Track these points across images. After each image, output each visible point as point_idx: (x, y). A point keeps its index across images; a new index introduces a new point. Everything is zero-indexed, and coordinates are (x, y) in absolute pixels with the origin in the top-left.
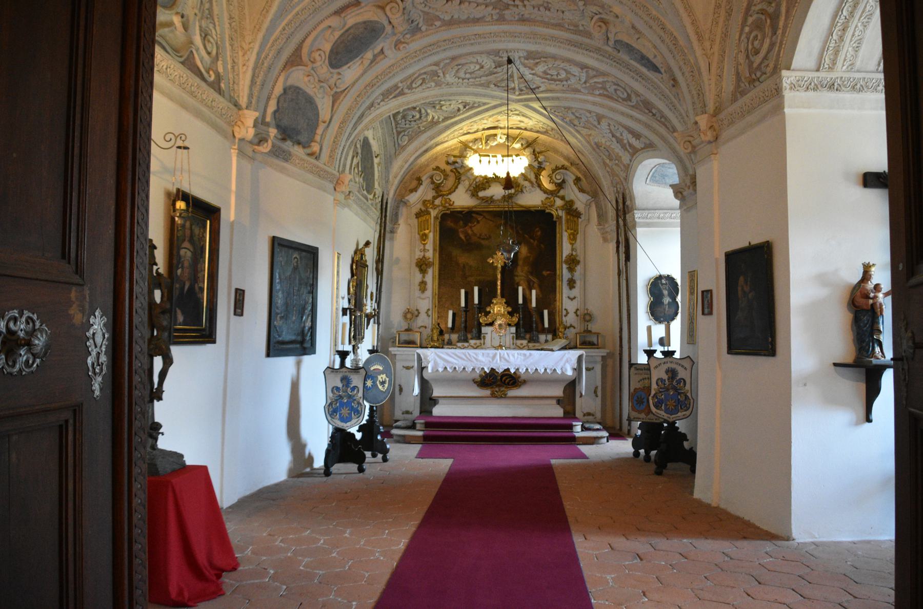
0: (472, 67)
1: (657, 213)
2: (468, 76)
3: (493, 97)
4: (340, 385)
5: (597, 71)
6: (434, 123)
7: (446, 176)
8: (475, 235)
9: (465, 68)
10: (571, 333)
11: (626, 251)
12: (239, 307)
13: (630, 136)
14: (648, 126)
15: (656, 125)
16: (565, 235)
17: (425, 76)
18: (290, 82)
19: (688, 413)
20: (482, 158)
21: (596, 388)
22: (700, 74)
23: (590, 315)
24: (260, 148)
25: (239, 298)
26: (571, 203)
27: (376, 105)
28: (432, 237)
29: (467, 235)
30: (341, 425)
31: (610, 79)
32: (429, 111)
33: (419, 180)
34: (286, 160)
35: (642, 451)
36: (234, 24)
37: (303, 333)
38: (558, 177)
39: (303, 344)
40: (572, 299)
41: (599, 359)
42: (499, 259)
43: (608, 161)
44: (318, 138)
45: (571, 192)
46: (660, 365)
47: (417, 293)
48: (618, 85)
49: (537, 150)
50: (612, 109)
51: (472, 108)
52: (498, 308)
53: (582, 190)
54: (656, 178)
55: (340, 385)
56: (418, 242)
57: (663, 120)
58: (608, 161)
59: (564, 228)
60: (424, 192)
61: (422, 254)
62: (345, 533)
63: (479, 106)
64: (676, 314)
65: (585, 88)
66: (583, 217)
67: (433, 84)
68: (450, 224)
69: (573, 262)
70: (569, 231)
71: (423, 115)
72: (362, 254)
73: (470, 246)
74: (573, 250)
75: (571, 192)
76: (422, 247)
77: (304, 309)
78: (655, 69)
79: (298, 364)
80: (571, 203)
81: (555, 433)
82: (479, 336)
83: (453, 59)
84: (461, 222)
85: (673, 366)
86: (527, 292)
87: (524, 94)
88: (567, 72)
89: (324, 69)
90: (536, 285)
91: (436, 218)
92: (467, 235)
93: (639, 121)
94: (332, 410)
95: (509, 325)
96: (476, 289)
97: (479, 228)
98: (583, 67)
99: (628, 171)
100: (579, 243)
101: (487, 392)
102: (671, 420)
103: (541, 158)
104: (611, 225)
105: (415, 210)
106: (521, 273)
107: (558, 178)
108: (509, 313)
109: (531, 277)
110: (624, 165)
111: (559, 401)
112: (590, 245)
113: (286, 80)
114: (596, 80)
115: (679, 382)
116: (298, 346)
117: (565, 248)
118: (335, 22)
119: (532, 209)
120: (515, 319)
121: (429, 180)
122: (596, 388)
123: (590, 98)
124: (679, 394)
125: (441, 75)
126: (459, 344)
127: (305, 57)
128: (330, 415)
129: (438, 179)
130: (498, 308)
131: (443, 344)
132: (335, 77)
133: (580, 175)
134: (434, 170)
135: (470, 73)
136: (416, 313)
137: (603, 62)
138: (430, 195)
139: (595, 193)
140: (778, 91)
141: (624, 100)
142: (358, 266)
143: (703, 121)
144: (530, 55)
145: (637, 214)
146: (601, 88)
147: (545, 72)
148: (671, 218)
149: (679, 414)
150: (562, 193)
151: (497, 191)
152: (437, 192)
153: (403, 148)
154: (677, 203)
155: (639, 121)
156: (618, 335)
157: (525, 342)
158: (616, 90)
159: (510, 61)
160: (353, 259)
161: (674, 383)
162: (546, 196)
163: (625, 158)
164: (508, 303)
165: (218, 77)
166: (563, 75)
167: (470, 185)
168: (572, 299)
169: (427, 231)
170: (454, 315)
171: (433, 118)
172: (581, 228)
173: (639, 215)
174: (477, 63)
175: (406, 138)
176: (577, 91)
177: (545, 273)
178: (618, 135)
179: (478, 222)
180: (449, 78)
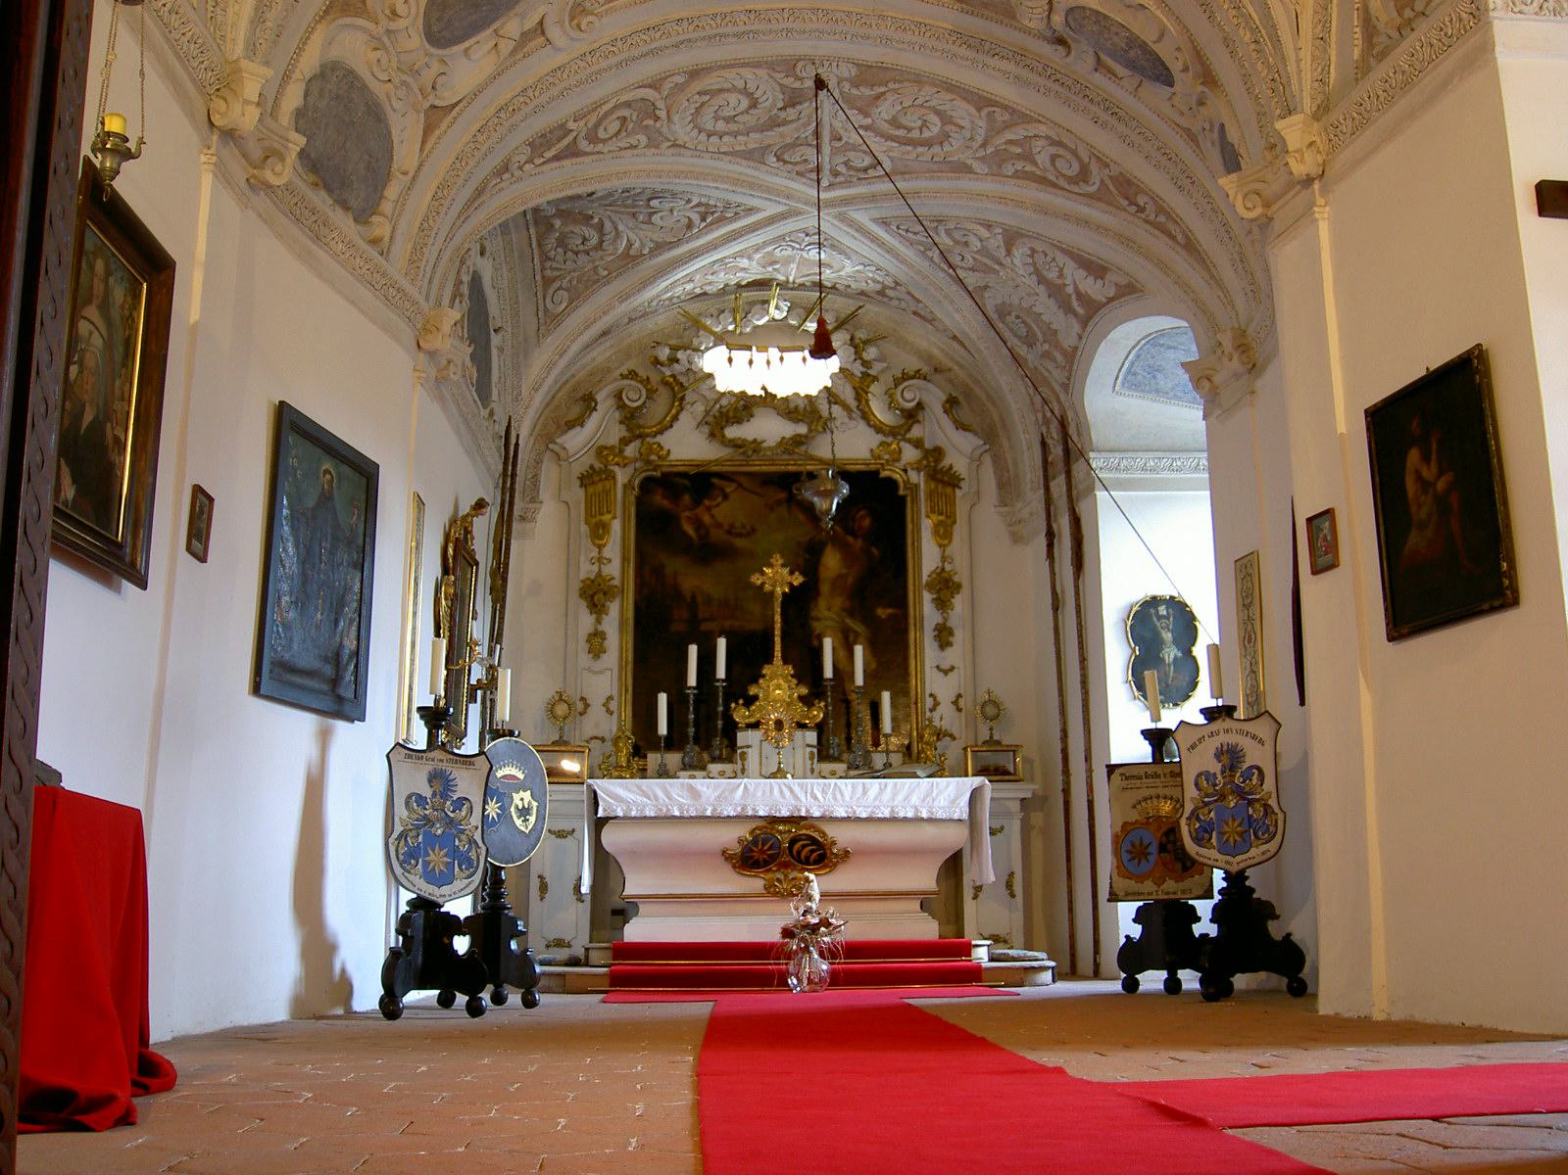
0: (733, 98)
1: (1141, 459)
2: (721, 126)
3: (769, 190)
4: (427, 792)
5: (1013, 111)
6: (630, 259)
7: (651, 393)
8: (720, 525)
9: (719, 100)
11: (1073, 549)
13: (1082, 273)
15: (1143, 235)
16: (927, 525)
17: (625, 113)
18: (334, 54)
19: (1272, 846)
20: (735, 354)
21: (1012, 874)
22: (1276, 41)
25: (201, 506)
27: (514, 167)
28: (619, 531)
29: (698, 524)
30: (430, 891)
31: (1043, 130)
32: (621, 227)
33: (589, 403)
34: (317, 238)
37: (336, 659)
38: (908, 395)
40: (946, 672)
41: (1015, 806)
42: (777, 577)
44: (387, 207)
45: (937, 429)
46: (1201, 740)
47: (585, 659)
48: (1060, 144)
49: (861, 335)
50: (1043, 210)
51: (722, 220)
52: (778, 687)
53: (961, 426)
54: (1139, 378)
55: (427, 792)
56: (587, 542)
57: (1164, 222)
59: (923, 508)
60: (602, 426)
61: (595, 568)
64: (1194, 685)
65: (982, 159)
67: (643, 139)
68: (659, 499)
69: (945, 587)
70: (935, 518)
72: (467, 532)
73: (708, 551)
74: (944, 559)
75: (937, 429)
76: (595, 553)
77: (341, 603)
79: (324, 738)
80: (938, 453)
83: (694, 74)
84: (687, 498)
88: (946, 119)
92: (698, 524)
93: (1101, 229)
95: (801, 726)
96: (722, 644)
97: (727, 510)
98: (982, 102)
99: (1074, 362)
100: (957, 547)
101: (755, 884)
105: (579, 467)
106: (827, 610)
107: (908, 397)
108: (801, 698)
109: (848, 621)
113: (329, 43)
114: (1009, 136)
115: (1247, 776)
117: (927, 555)
121: (611, 401)
123: (989, 186)
124: (1251, 803)
125: (663, 114)
129: (634, 397)
130: (778, 687)
132: (436, 67)
135: (728, 120)
136: (580, 706)
137: (1027, 83)
138: (615, 434)
139: (991, 435)
141: (1072, 180)
142: (457, 558)
144: (869, 74)
145: (1097, 461)
146: (1020, 157)
147: (894, 122)
148: (1170, 469)
149: (1253, 852)
150: (916, 432)
151: (769, 429)
152: (629, 430)
155: (1101, 229)
156: (1059, 746)
157: (841, 767)
158: (1053, 158)
159: (820, 84)
160: (447, 537)
161: (1238, 780)
162: (880, 438)
163: (1067, 328)
164: (799, 678)
166: (935, 127)
167: (707, 413)
168: (946, 672)
169: (607, 517)
171: (630, 245)
172: (961, 509)
173: (1100, 464)
174: (745, 92)
176: (963, 169)
177: (882, 612)
178: (1052, 275)
179: (726, 497)
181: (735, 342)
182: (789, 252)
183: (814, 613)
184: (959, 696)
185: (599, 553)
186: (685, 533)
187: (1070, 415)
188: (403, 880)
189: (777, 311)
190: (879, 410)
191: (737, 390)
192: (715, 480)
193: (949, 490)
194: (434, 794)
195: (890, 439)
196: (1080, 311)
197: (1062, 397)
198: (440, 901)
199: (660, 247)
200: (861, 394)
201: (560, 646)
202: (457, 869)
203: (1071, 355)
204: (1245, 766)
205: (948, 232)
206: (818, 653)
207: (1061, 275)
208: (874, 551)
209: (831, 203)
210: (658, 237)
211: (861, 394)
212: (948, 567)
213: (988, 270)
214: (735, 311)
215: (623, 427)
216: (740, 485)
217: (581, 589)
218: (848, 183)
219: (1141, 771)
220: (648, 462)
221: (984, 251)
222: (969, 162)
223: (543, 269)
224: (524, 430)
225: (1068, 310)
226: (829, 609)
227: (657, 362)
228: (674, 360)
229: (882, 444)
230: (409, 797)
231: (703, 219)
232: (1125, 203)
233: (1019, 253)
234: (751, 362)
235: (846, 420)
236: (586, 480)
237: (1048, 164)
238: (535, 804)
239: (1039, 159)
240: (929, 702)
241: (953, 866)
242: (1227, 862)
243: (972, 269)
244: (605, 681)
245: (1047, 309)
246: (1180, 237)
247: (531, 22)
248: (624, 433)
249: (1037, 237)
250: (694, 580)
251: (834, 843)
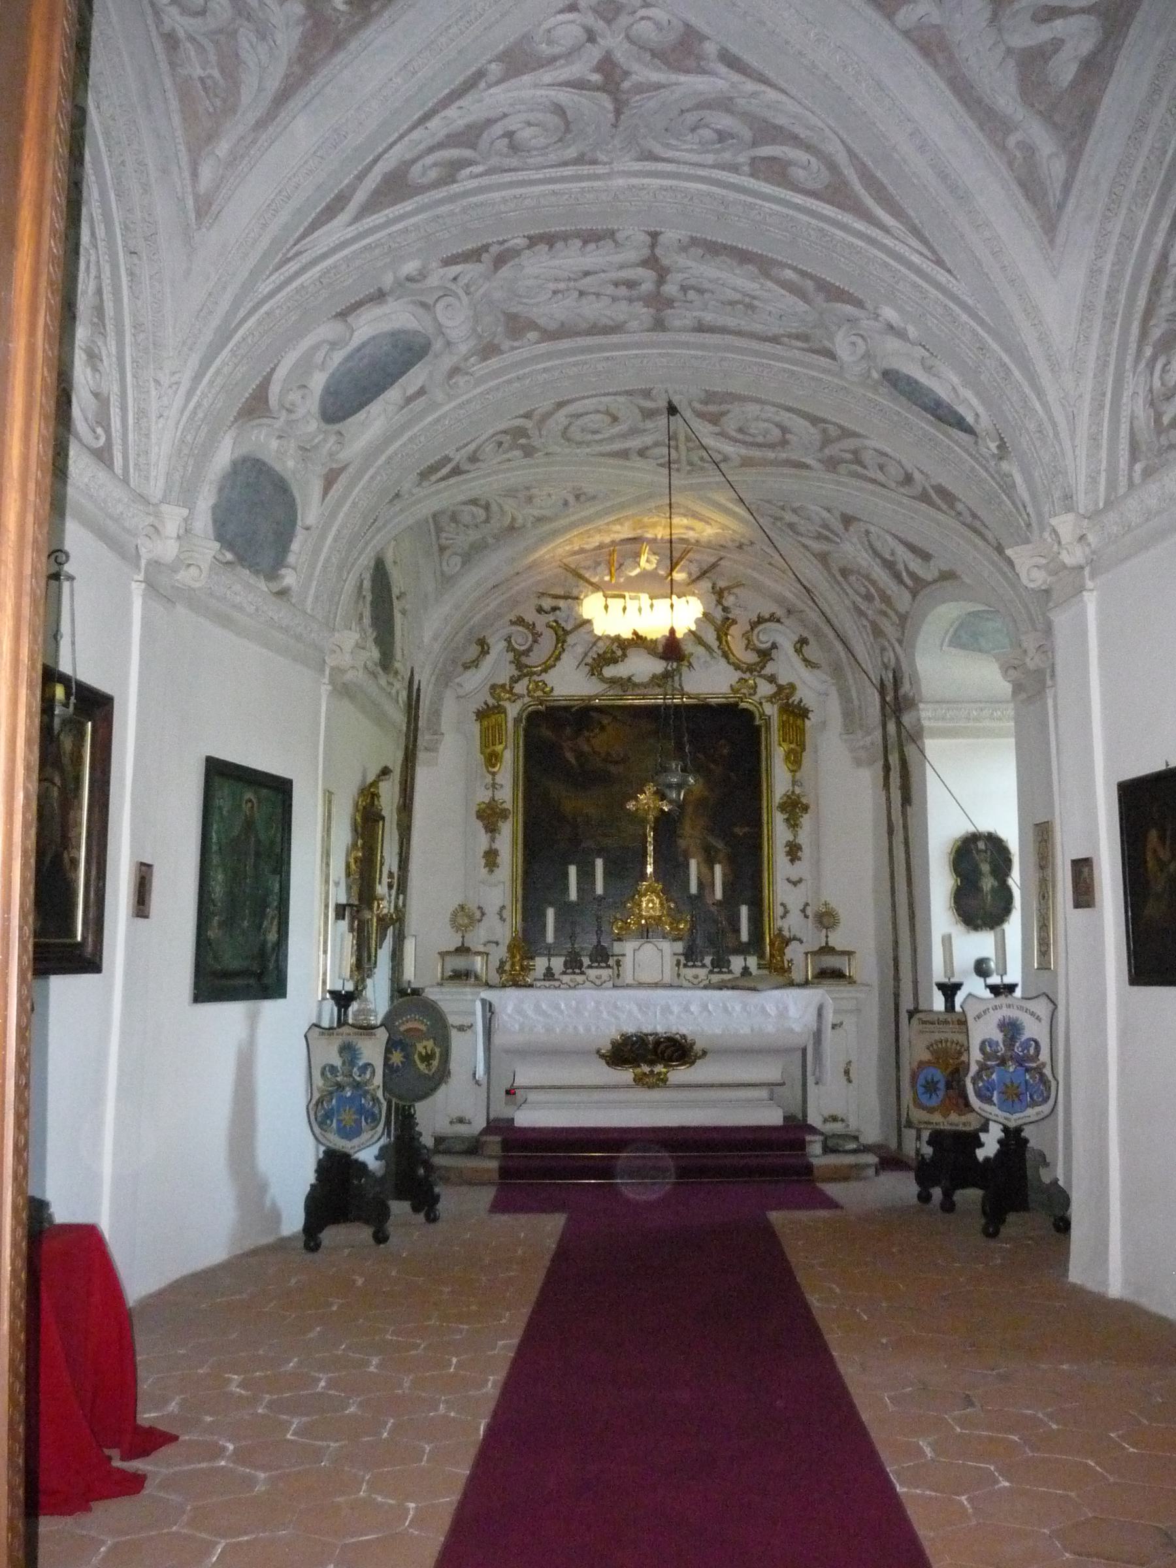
4: (337, 1062)
7: (536, 636)
16: (779, 753)
19: (1045, 1109)
29: (580, 755)
30: (340, 1144)
32: (506, 508)
33: (484, 647)
36: (142, 336)
40: (795, 884)
49: (722, 584)
55: (337, 1062)
58: (864, 606)
60: (496, 667)
61: (489, 793)
62: (367, 1363)
64: (1007, 910)
68: (546, 733)
69: (794, 807)
70: (786, 746)
72: (374, 796)
73: (588, 777)
74: (794, 783)
76: (489, 779)
79: (253, 1020)
85: (1014, 1013)
86: (705, 870)
91: (517, 721)
92: (580, 755)
94: (322, 1114)
101: (626, 1075)
102: (1012, 1124)
103: (729, 601)
105: (477, 704)
115: (1025, 1045)
116: (252, 981)
117: (779, 780)
121: (504, 644)
127: (273, 401)
133: (805, 635)
134: (512, 623)
136: (478, 914)
142: (367, 820)
145: (926, 714)
148: (992, 718)
150: (769, 669)
151: (642, 667)
154: (1005, 688)
159: (672, 410)
162: (738, 674)
168: (795, 884)
169: (499, 748)
171: (513, 519)
173: (929, 714)
177: (739, 831)
179: (603, 728)
181: (612, 591)
182: (655, 519)
184: (807, 904)
185: (493, 779)
189: (647, 562)
191: (612, 635)
192: (593, 714)
193: (799, 722)
194: (344, 1063)
195: (747, 676)
198: (352, 1152)
201: (458, 867)
202: (364, 1123)
203: (903, 618)
204: (1024, 1038)
207: (893, 554)
210: (536, 512)
212: (798, 790)
214: (612, 566)
215: (513, 666)
216: (615, 718)
217: (478, 811)
223: (438, 538)
224: (425, 678)
225: (901, 581)
229: (741, 679)
230: (324, 1068)
234: (624, 609)
235: (708, 659)
236: (481, 715)
240: (780, 911)
242: (1006, 1118)
244: (499, 892)
245: (881, 575)
250: (574, 803)
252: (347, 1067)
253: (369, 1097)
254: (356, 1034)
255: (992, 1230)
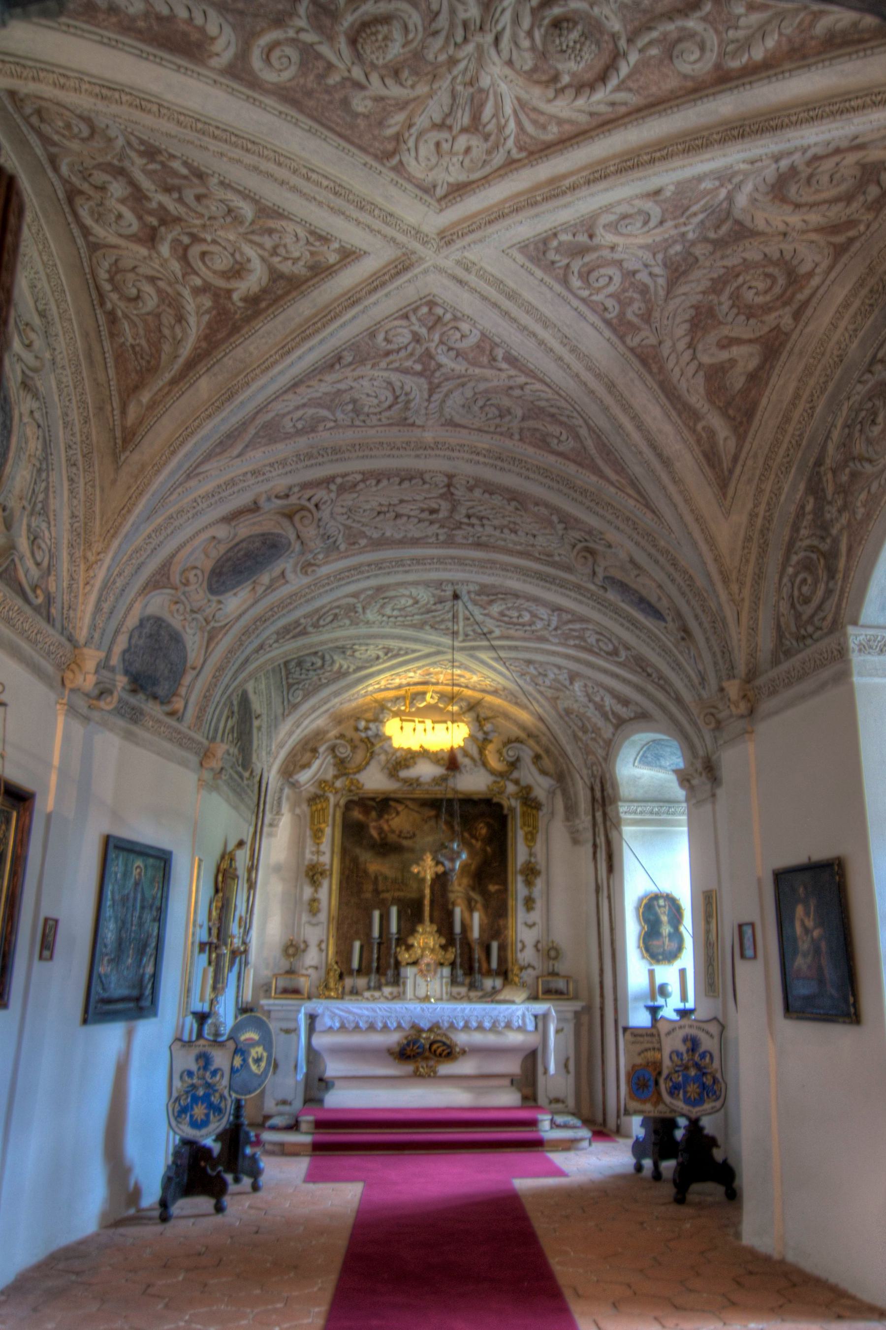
0: (403, 601)
2: (396, 613)
3: (426, 642)
4: (194, 1067)
6: (342, 674)
8: (393, 832)
10: (528, 975)
12: (47, 944)
14: (641, 690)
15: (650, 688)
16: (521, 834)
17: (337, 611)
20: (405, 724)
23: (557, 950)
24: (102, 704)
26: (529, 788)
27: (266, 647)
28: (331, 834)
31: (590, 626)
32: (335, 657)
35: (648, 1163)
39: (139, 1003)
41: (570, 1016)
43: (580, 734)
44: (183, 691)
45: (529, 774)
48: (601, 634)
49: (482, 715)
52: (426, 939)
53: (543, 772)
54: (649, 757)
55: (194, 1067)
58: (580, 734)
59: (519, 822)
63: (406, 654)
64: (680, 948)
65: (555, 636)
66: (545, 809)
68: (357, 814)
69: (531, 872)
70: (526, 829)
71: (328, 663)
73: (386, 848)
74: (531, 855)
75: (529, 774)
77: (145, 945)
78: (657, 614)
79: (130, 1035)
80: (529, 788)
81: (511, 1136)
82: (397, 980)
83: (379, 589)
84: (374, 814)
86: (466, 915)
87: (470, 640)
88: (534, 615)
89: (198, 594)
90: (479, 906)
91: (337, 805)
92: (381, 830)
93: (625, 681)
94: (181, 1110)
95: (442, 964)
96: (394, 910)
97: (399, 822)
99: (610, 749)
100: (539, 847)
101: (409, 1068)
103: (488, 727)
104: (584, 820)
110: (604, 740)
111: (513, 1081)
112: (551, 849)
114: (571, 626)
116: (132, 1005)
117: (520, 853)
118: (222, 532)
119: (475, 797)
120: (450, 955)
122: (567, 1059)
125: (360, 610)
126: (367, 994)
127: (176, 578)
128: (176, 1119)
129: (344, 751)
130: (426, 939)
131: (343, 993)
133: (540, 751)
134: (337, 738)
135: (400, 610)
138: (331, 772)
140: (841, 654)
141: (608, 653)
143: (733, 689)
145: (623, 808)
146: (577, 637)
147: (502, 614)
148: (668, 813)
150: (515, 775)
151: (426, 771)
153: (295, 706)
154: (681, 794)
155: (625, 681)
156: (597, 979)
157: (463, 990)
158: (598, 641)
159: (456, 597)
164: (439, 932)
165: (49, 599)
166: (527, 617)
167: (388, 761)
169: (323, 826)
170: (362, 947)
171: (341, 667)
172: (542, 824)
174: (411, 596)
175: (300, 693)
176: (542, 639)
177: (492, 888)
178: (598, 699)
179: (398, 813)
180: (371, 615)
182: (439, 669)
183: (450, 888)
184: (538, 942)
186: (371, 837)
187: (608, 776)
188: (176, 1129)
190: (493, 761)
192: (392, 803)
193: (534, 812)
194: (199, 1069)
195: (499, 779)
196: (614, 721)
197: (604, 765)
199: (359, 669)
200: (481, 751)
203: (609, 743)
205: (535, 668)
206: (450, 914)
207: (602, 699)
208: (488, 849)
209: (462, 649)
211: (481, 751)
212: (533, 860)
213: (557, 690)
216: (407, 806)
218: (474, 640)
219: (644, 1032)
220: (350, 791)
221: (556, 680)
222: (547, 636)
223: (287, 678)
226: (460, 885)
227: (357, 729)
228: (367, 729)
229: (495, 782)
231: (386, 654)
232: (639, 670)
233: (577, 686)
237: (594, 643)
238: (265, 1054)
239: (589, 640)
240: (519, 946)
241: (532, 1059)
243: (550, 687)
246: (672, 694)
247: (277, 572)
248: (336, 773)
249: (589, 678)
251: (456, 1045)
252: (201, 1072)
253: (217, 1095)
254: (210, 1046)
255: (680, 1199)
